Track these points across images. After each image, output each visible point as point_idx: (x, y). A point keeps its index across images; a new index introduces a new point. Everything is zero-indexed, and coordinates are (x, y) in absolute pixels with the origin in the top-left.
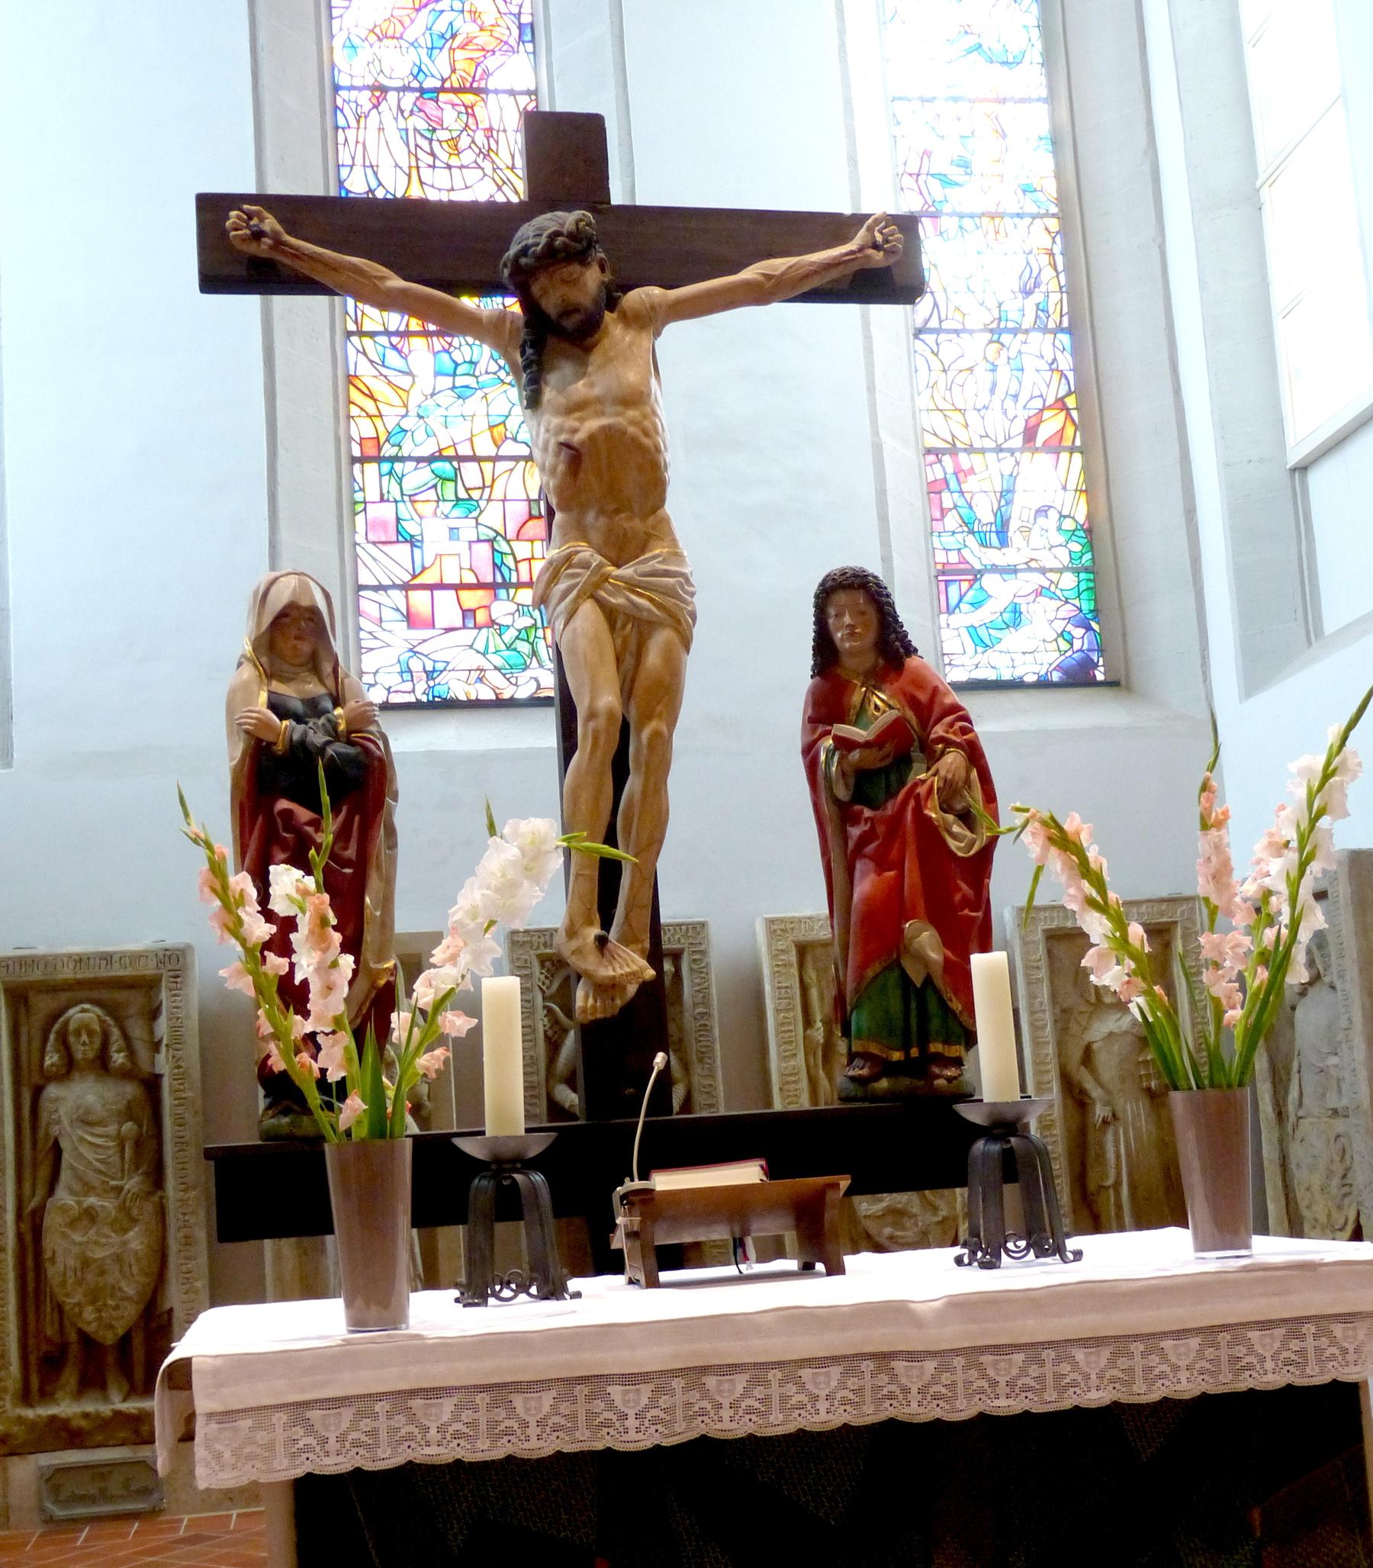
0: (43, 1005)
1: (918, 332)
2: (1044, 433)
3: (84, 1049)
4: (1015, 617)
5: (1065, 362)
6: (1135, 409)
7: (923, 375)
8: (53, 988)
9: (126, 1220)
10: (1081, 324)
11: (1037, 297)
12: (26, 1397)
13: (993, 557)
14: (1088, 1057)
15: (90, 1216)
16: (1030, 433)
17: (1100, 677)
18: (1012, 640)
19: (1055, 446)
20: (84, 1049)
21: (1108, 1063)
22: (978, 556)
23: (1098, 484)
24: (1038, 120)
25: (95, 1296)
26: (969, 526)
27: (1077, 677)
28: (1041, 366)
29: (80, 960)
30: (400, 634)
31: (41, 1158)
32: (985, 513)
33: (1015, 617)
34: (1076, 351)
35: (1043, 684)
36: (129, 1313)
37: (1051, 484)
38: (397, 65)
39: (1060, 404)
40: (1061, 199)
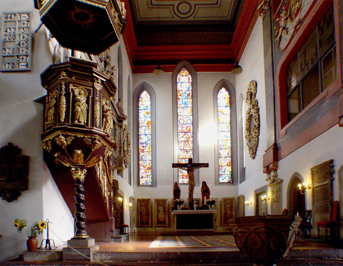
0: (159, 202)
1: (219, 158)
2: (228, 165)
3: (161, 205)
4: (225, 178)
5: (230, 159)
6: (235, 164)
7: (219, 161)
8: (159, 201)
9: (163, 215)
10: (232, 157)
11: (229, 155)
12: (157, 224)
13: (224, 174)
14: (226, 208)
15: (161, 214)
16: (227, 165)
17: (231, 182)
18: (225, 179)
19: (229, 166)
20: (161, 205)
21: (228, 208)
22: (222, 174)
23: (232, 168)
24: (230, 142)
25: (161, 219)
26: (222, 171)
27: (229, 182)
28: (229, 160)
29: (161, 199)
30: (182, 179)
31: (158, 211)
32: (223, 171)
33: (225, 178)
34: (231, 159)
35: (227, 183)
36: (163, 220)
37: (229, 169)
38: (183, 139)
39: (230, 162)
40: (231, 147)
